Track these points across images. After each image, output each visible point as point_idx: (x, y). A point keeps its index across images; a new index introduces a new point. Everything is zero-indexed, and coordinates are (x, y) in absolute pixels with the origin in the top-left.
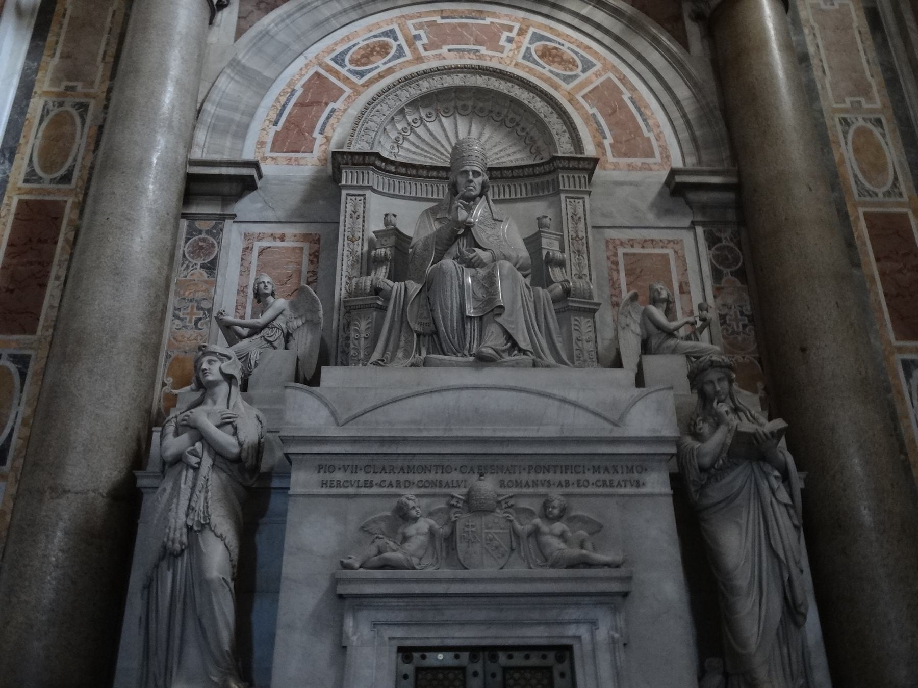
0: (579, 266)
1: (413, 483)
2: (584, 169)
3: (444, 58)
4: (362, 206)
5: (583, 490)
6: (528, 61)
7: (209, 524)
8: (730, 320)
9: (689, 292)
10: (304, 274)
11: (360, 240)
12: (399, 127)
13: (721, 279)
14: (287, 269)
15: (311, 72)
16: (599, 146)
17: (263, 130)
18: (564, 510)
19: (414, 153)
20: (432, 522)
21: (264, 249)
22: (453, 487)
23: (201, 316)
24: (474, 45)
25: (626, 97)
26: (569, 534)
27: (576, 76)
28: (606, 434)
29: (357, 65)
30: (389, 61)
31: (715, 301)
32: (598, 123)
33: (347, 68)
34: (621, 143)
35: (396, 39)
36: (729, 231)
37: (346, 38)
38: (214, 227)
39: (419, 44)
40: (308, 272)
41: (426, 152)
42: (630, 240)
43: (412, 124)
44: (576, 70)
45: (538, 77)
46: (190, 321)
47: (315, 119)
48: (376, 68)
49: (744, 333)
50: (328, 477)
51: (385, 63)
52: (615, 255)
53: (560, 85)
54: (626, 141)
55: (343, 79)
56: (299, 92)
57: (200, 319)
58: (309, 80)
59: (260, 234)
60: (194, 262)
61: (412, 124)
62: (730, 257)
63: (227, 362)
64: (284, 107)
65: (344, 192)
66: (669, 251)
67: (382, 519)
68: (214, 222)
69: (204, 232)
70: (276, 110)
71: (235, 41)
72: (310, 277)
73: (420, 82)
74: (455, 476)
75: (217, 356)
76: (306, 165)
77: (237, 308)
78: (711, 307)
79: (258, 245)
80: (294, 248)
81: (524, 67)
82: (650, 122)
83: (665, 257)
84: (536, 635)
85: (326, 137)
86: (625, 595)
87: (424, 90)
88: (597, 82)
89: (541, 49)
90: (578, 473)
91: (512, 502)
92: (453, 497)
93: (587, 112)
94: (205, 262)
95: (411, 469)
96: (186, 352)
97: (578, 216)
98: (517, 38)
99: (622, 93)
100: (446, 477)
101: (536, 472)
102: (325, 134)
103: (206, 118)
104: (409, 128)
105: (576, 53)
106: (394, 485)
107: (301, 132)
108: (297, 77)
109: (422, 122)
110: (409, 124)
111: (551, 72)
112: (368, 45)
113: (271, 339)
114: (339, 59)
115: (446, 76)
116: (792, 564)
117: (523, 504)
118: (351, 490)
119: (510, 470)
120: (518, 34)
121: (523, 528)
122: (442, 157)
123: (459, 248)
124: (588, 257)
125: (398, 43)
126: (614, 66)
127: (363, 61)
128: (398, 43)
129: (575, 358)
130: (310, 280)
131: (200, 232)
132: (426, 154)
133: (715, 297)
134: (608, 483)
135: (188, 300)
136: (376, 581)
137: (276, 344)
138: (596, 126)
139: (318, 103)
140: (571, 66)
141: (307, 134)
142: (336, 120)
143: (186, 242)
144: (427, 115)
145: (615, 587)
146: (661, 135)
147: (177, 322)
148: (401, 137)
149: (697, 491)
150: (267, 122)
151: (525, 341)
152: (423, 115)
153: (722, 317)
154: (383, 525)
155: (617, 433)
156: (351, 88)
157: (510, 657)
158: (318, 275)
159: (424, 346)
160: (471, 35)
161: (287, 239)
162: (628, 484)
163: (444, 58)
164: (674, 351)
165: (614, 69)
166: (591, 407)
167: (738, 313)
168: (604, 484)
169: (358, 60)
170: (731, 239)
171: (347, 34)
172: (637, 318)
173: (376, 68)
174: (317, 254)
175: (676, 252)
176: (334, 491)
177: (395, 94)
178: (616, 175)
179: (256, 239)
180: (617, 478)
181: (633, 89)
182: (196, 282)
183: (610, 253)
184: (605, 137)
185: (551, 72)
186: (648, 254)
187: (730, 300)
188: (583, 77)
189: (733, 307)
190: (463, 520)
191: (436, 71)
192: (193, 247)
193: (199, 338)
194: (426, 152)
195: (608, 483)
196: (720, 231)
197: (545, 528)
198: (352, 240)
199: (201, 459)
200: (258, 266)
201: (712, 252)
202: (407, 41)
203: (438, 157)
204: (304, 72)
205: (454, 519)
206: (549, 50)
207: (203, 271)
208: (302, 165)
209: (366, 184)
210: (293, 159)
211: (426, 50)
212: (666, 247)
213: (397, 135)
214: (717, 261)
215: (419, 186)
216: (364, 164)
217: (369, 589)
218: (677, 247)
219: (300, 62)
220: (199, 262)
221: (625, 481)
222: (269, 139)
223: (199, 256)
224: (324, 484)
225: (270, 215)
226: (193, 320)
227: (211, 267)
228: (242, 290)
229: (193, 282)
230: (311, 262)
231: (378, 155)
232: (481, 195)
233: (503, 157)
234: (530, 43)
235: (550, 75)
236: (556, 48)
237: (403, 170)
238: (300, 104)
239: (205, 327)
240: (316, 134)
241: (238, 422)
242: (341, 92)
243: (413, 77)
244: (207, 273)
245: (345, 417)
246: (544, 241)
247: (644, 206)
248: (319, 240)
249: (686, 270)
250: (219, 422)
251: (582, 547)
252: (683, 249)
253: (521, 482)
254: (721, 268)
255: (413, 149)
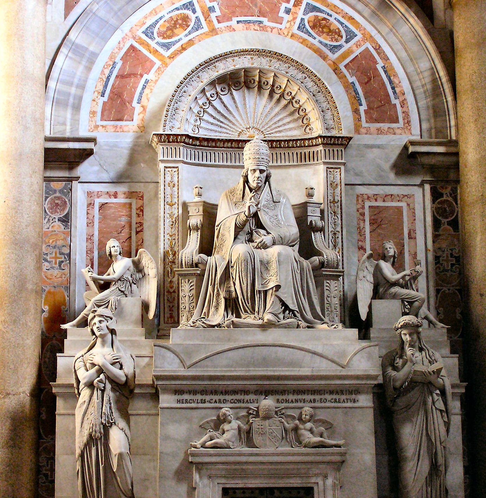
0: (335, 224)
1: (228, 401)
2: (342, 144)
3: (234, 30)
4: (177, 176)
5: (323, 405)
6: (302, 32)
7: (115, 423)
8: (443, 260)
9: (415, 238)
10: (134, 226)
11: (176, 205)
12: (201, 102)
13: (440, 227)
14: (120, 221)
15: (127, 46)
16: (355, 112)
17: (94, 100)
18: (312, 416)
19: (212, 124)
20: (239, 422)
21: (103, 205)
22: (250, 403)
23: (63, 260)
24: (258, 16)
25: (379, 67)
26: (315, 429)
27: (340, 46)
28: (338, 373)
29: (164, 38)
30: (190, 33)
31: (434, 245)
32: (356, 92)
33: (156, 41)
34: (373, 109)
35: (194, 11)
36: (450, 188)
37: (154, 12)
38: (65, 188)
39: (213, 16)
40: (136, 223)
41: (222, 122)
42: (374, 195)
43: (211, 98)
44: (340, 40)
45: (309, 48)
46: (56, 263)
47: (133, 89)
48: (179, 40)
49: (451, 271)
50: (180, 397)
51: (186, 36)
52: (363, 207)
53: (328, 56)
54: (376, 108)
55: (154, 52)
56: (118, 67)
57: (62, 262)
58: (126, 53)
59: (98, 192)
60: (53, 216)
61: (211, 98)
62: (447, 209)
63: (110, 321)
64: (108, 79)
65: (162, 166)
66: (403, 204)
67: (212, 420)
68: (64, 183)
69: (57, 191)
70: (102, 82)
71: (65, 18)
72: (139, 227)
73: (217, 64)
74: (252, 397)
75: (104, 318)
76: (129, 132)
77: (87, 253)
78: (430, 250)
79: (98, 202)
80: (125, 204)
81: (299, 38)
82: (397, 90)
83: (399, 210)
84: (295, 482)
85: (143, 106)
86: (343, 462)
87: (221, 72)
88: (357, 52)
89: (313, 20)
90: (321, 395)
91: (283, 411)
92: (250, 409)
93: (347, 81)
94: (60, 216)
95: (227, 393)
96: (55, 287)
97: (335, 183)
98: (293, 10)
99: (376, 63)
100: (247, 397)
101: (298, 394)
102: (142, 103)
103: (51, 94)
104: (208, 102)
105: (342, 24)
106: (217, 401)
107: (123, 103)
108: (117, 50)
109: (217, 96)
110: (208, 99)
111: (321, 42)
112: (171, 17)
113: (123, 289)
114: (149, 33)
115: (236, 58)
116: (438, 443)
117: (290, 412)
118: (193, 405)
119: (283, 392)
120: (294, 5)
121: (289, 426)
122: (234, 127)
123: (250, 226)
124: (341, 217)
125: (196, 15)
126: (371, 37)
127: (169, 33)
128: (196, 15)
129: (326, 310)
130: (138, 230)
131: (55, 192)
132: (221, 124)
133: (434, 242)
134: (337, 400)
135: (52, 246)
136: (211, 455)
137: (126, 292)
138: (354, 94)
139: (135, 75)
140: (336, 36)
141: (127, 103)
142: (150, 91)
143: (46, 200)
144: (221, 89)
145: (338, 458)
146: (405, 102)
147: (46, 264)
148: (202, 110)
149: (391, 401)
150: (96, 93)
151: (293, 303)
152: (219, 90)
153: (437, 258)
154: (212, 424)
155: (344, 373)
156: (160, 60)
157: (281, 492)
158: (144, 225)
159: (230, 307)
160: (256, 6)
161: (119, 196)
162: (349, 401)
163: (234, 30)
164: (394, 296)
165: (371, 39)
166: (330, 357)
167: (449, 256)
168: (335, 401)
169: (165, 33)
170: (451, 195)
171: (154, 7)
172: (372, 270)
173: (179, 40)
174: (142, 208)
175: (408, 205)
176: (184, 405)
177: (197, 76)
178: (367, 139)
179: (96, 197)
180: (343, 397)
181: (386, 58)
182: (56, 232)
183: (359, 206)
184: (361, 105)
185: (321, 42)
186: (387, 207)
187: (444, 245)
188: (346, 46)
189: (446, 250)
190: (256, 423)
191: (229, 54)
192: (51, 204)
193: (63, 276)
194: (222, 122)
195: (337, 400)
196: (442, 187)
197: (301, 426)
198: (171, 205)
199: (105, 384)
200: (99, 218)
201: (434, 205)
202: (203, 13)
203: (230, 127)
204: (121, 46)
205: (251, 421)
206: (319, 21)
207: (59, 223)
208: (126, 132)
209: (178, 159)
210: (119, 126)
211: (219, 22)
212: (401, 201)
213: (199, 109)
214: (438, 213)
215: (217, 154)
216: (177, 142)
217: (207, 459)
218: (409, 201)
219: (118, 36)
220: (57, 216)
221: (347, 399)
222: (99, 109)
223: (56, 212)
224: (178, 401)
225: (105, 177)
226: (58, 263)
227: (66, 220)
228: (90, 238)
229: (54, 233)
230: (138, 215)
231: (188, 136)
232: (265, 183)
233: (281, 126)
234: (304, 14)
235: (318, 45)
236: (324, 19)
237: (206, 144)
238: (121, 76)
239: (66, 268)
240: (135, 104)
241: (122, 361)
242: (153, 64)
243: (211, 61)
244: (64, 225)
245: (188, 363)
246: (309, 209)
247: (387, 166)
248: (142, 197)
249: (415, 220)
250: (112, 362)
251: (321, 437)
252: (414, 203)
253: (288, 400)
254: (440, 218)
255: (211, 120)
